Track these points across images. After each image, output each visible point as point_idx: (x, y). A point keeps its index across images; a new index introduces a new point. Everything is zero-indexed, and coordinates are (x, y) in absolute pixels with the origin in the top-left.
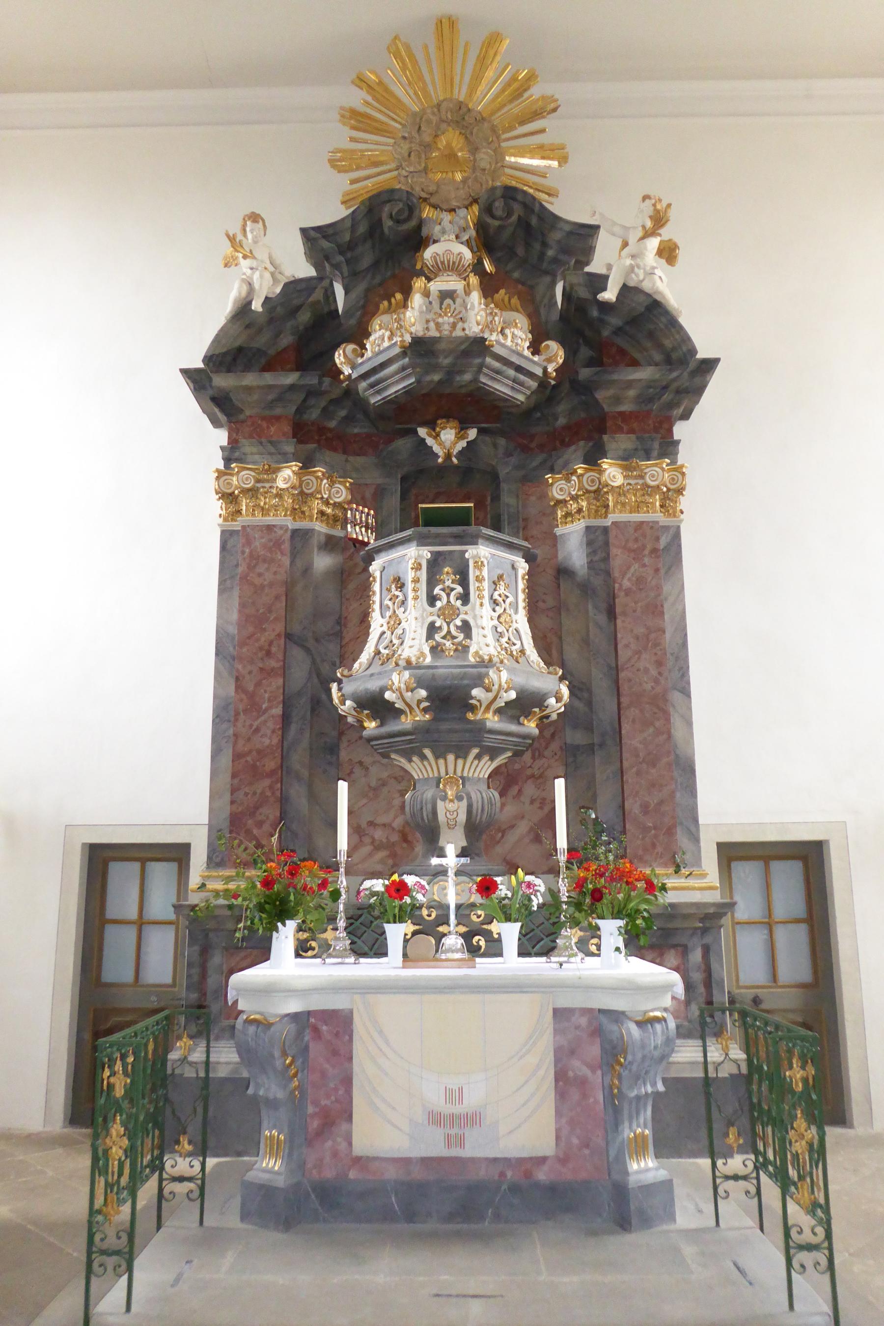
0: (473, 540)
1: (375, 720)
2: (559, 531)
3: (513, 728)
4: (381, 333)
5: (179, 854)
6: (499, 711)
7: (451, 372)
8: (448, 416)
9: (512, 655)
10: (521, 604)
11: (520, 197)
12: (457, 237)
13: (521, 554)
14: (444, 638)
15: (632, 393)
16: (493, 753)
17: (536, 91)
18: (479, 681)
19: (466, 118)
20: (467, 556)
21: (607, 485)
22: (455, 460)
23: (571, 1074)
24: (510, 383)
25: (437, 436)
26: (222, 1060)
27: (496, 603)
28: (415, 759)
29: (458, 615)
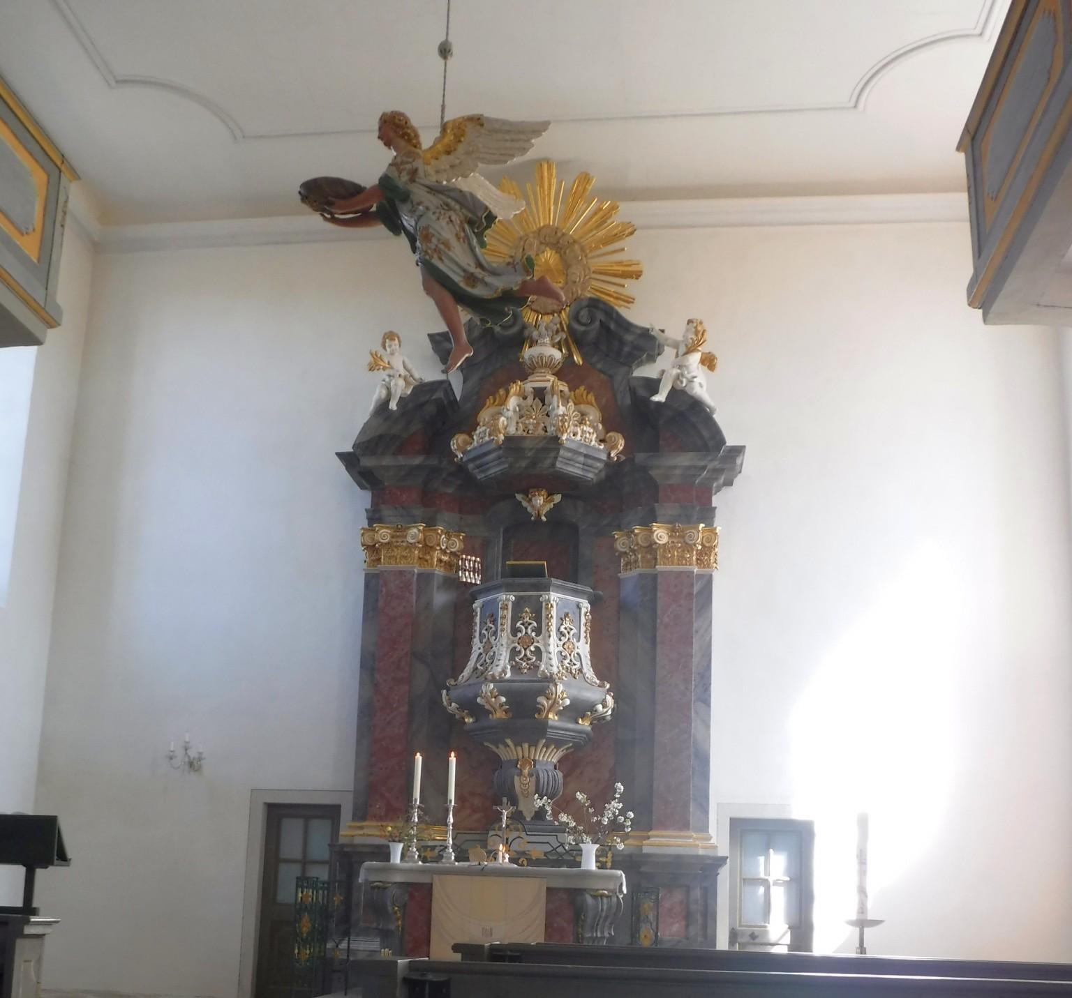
0: (546, 588)
1: (472, 717)
2: (622, 575)
3: (571, 726)
4: (484, 428)
5: (330, 813)
6: (559, 713)
7: (534, 463)
8: (538, 487)
9: (571, 673)
10: (583, 635)
11: (601, 306)
12: (552, 339)
13: (586, 596)
14: (521, 659)
15: (678, 472)
16: (558, 743)
17: (616, 220)
18: (543, 692)
19: (561, 242)
20: (541, 599)
21: (656, 543)
22: (544, 518)
23: (555, 925)
24: (581, 466)
25: (530, 500)
26: (361, 948)
27: (562, 634)
28: (501, 746)
29: (533, 643)
